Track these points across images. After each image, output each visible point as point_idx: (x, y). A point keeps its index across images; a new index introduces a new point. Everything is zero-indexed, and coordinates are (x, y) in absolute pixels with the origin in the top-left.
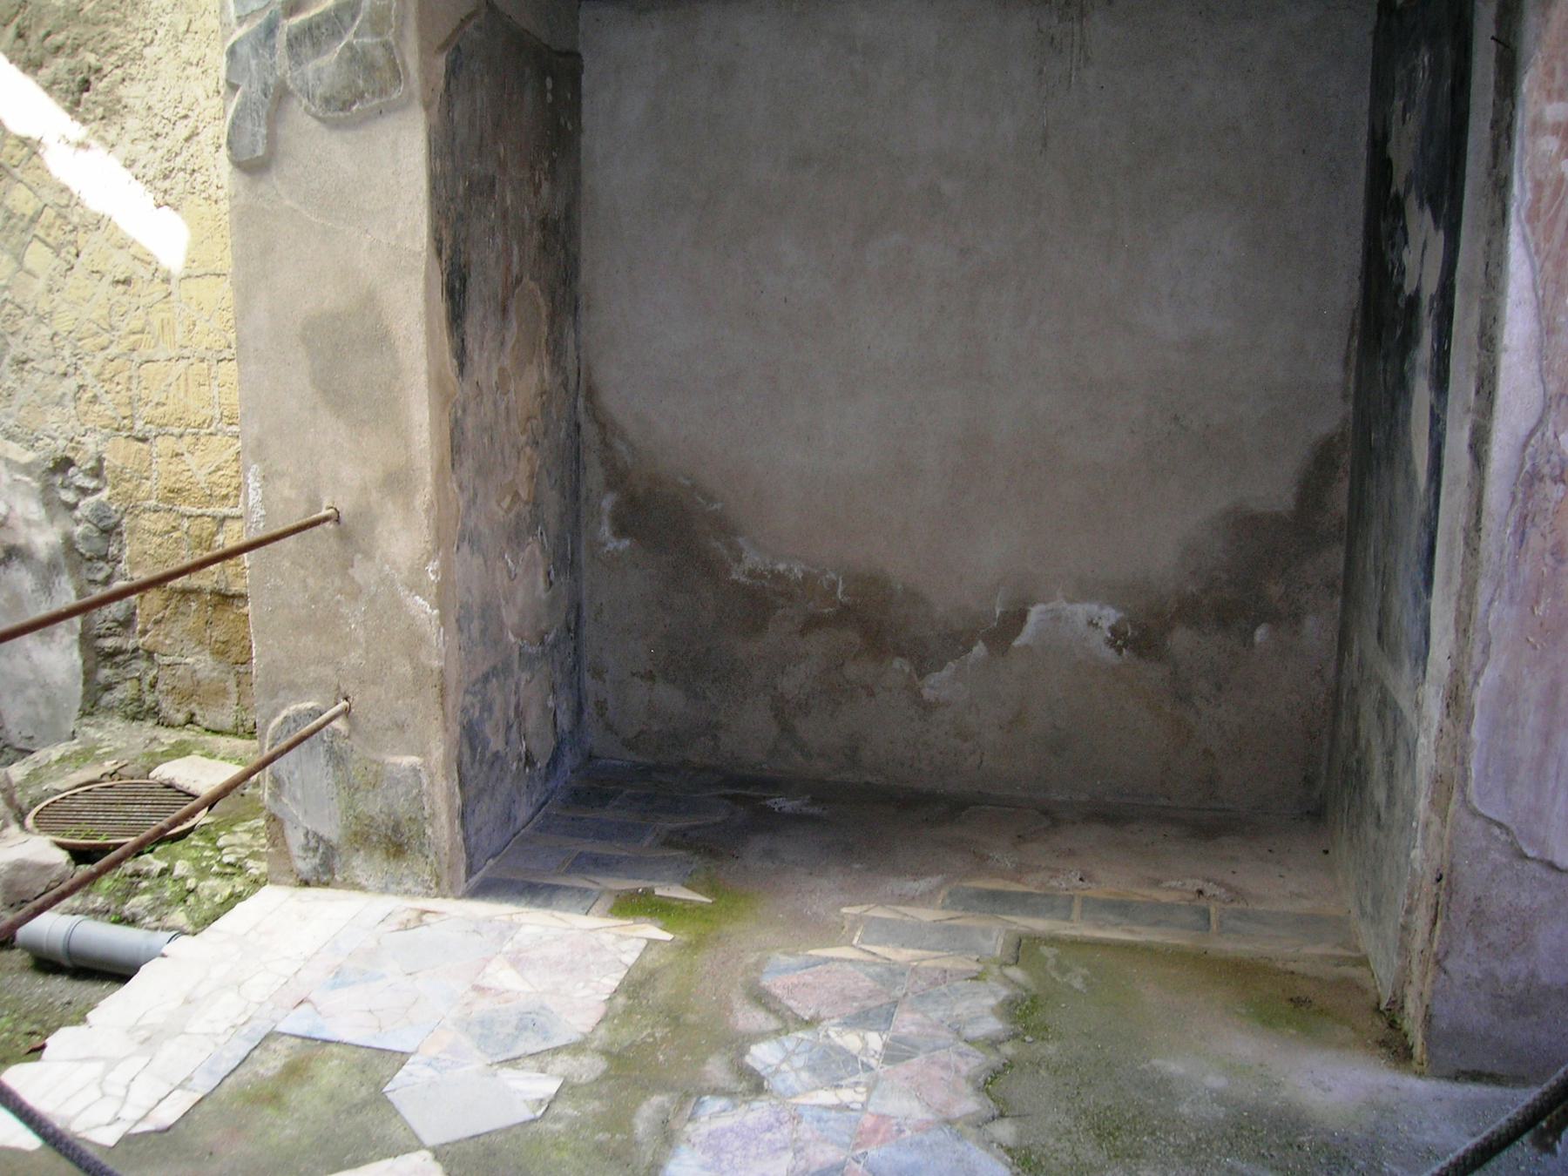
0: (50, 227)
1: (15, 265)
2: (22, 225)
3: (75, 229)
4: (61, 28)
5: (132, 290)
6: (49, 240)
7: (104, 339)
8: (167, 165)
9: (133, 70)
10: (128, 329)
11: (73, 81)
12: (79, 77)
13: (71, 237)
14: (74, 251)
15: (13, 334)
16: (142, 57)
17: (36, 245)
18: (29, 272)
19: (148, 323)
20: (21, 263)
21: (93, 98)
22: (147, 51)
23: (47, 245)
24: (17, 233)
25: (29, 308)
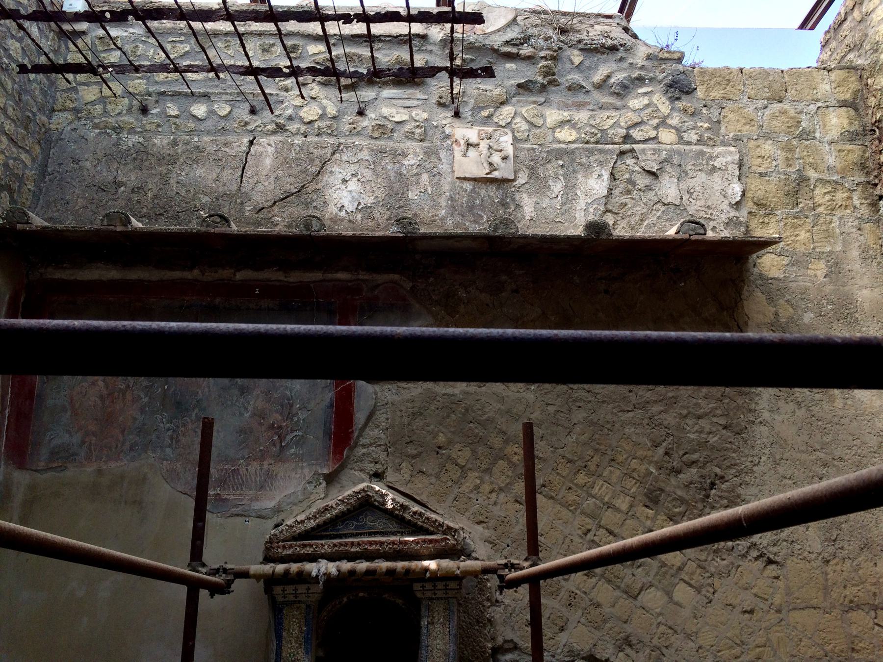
0: (693, 573)
1: (666, 598)
2: (672, 571)
3: (712, 575)
4: (695, 451)
5: (755, 617)
6: (692, 582)
7: (737, 651)
8: (775, 537)
9: (747, 479)
10: (754, 644)
11: (705, 483)
12: (709, 481)
13: (709, 581)
14: (712, 590)
15: (666, 647)
16: (752, 472)
17: (682, 585)
18: (677, 604)
19: (768, 640)
20: (671, 598)
21: (719, 494)
22: (755, 468)
23: (690, 585)
24: (668, 577)
25: (679, 629)
